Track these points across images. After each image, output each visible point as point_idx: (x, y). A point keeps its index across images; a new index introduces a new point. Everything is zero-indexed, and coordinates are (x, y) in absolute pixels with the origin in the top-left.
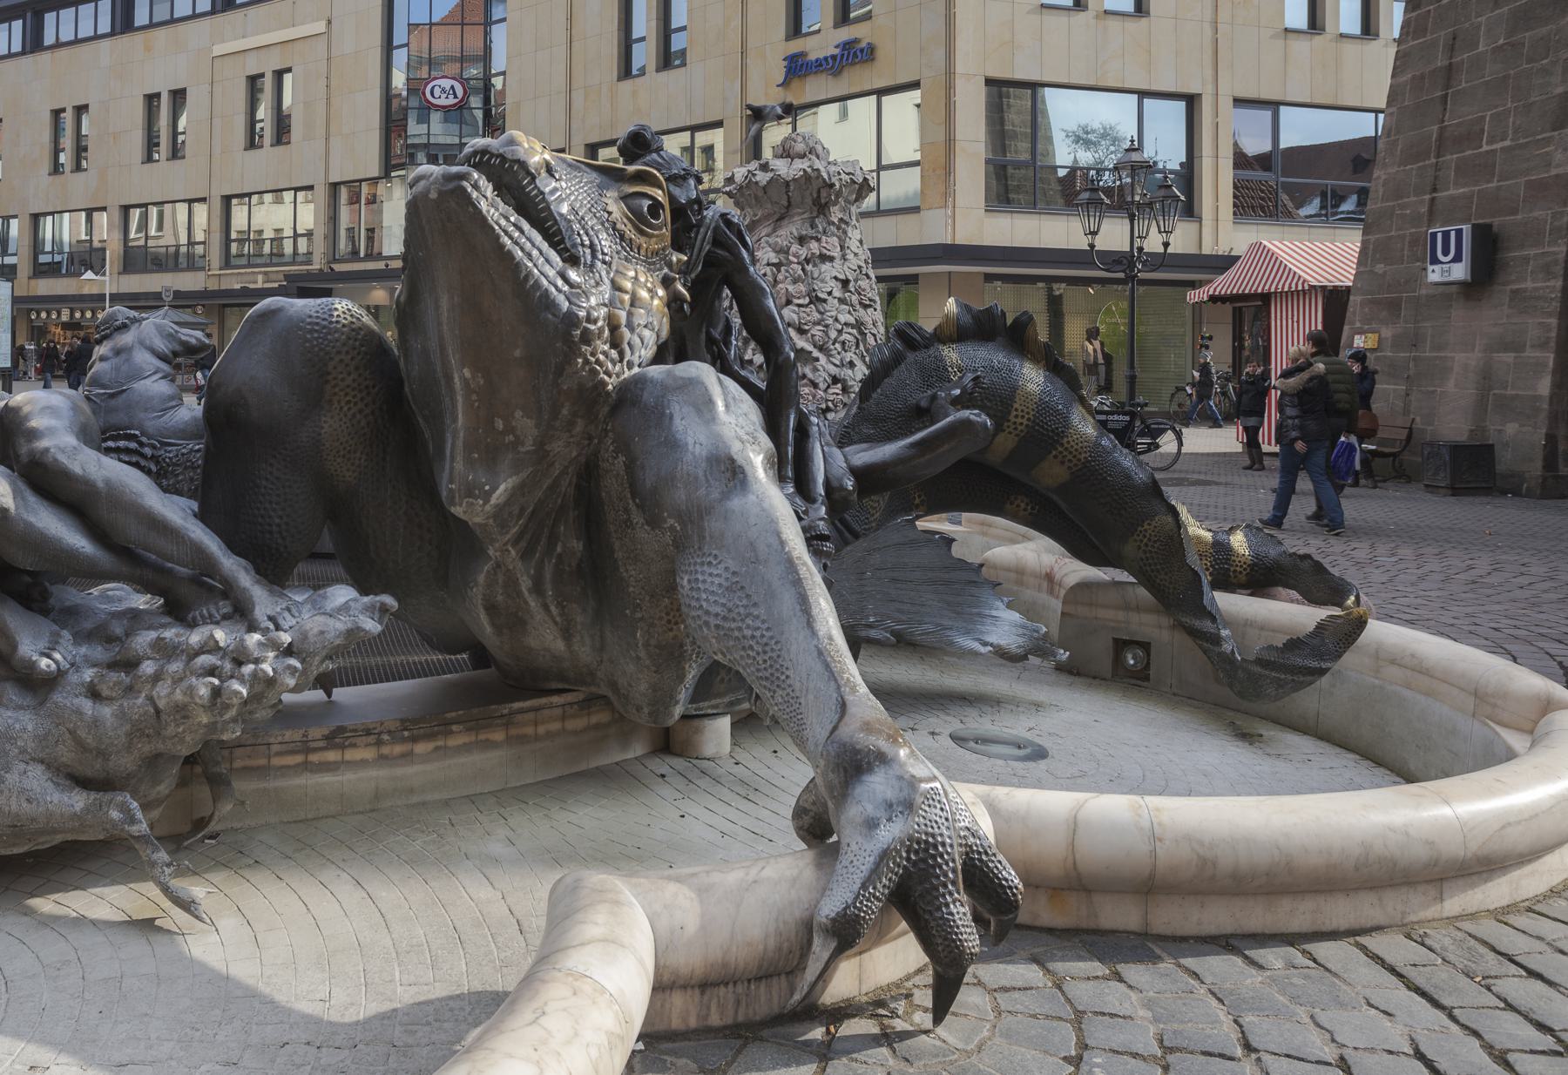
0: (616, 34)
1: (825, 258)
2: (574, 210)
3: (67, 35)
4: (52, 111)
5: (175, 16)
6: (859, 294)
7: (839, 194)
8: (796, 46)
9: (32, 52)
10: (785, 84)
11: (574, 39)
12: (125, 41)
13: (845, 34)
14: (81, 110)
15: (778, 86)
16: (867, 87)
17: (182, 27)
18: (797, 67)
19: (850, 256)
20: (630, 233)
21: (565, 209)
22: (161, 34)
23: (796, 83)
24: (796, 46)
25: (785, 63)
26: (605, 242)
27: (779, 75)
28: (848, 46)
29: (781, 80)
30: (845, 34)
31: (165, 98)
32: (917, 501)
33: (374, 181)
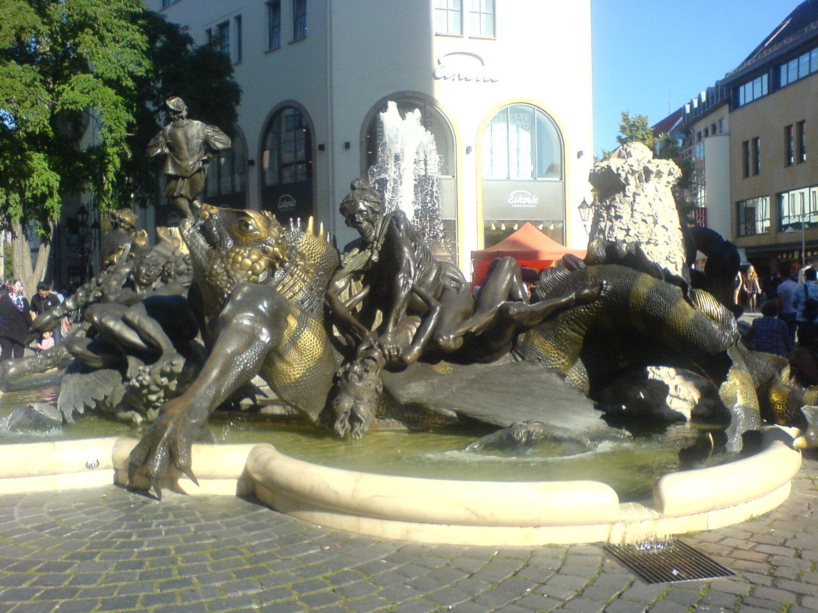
1: (618, 217)
3: (793, 77)
6: (638, 237)
9: (773, 92)
14: (801, 124)
19: (636, 214)
32: (621, 357)
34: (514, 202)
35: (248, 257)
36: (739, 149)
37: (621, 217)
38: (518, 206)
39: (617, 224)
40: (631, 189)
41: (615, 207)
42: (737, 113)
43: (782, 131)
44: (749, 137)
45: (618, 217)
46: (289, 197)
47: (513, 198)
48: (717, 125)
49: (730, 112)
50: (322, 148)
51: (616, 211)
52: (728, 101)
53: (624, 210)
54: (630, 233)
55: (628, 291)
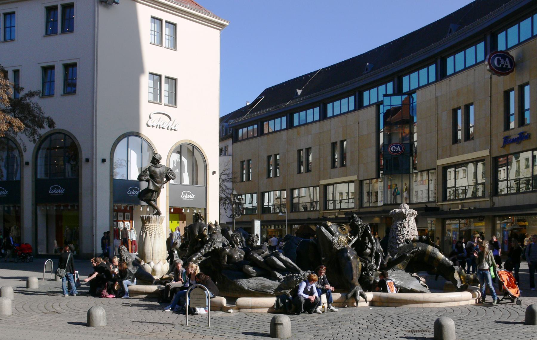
0: (451, 128)
1: (404, 227)
2: (334, 230)
3: (272, 129)
4: (267, 156)
5: (307, 122)
7: (407, 216)
8: (507, 133)
10: (504, 146)
11: (438, 129)
12: (291, 131)
13: (521, 130)
15: (501, 147)
16: (528, 148)
17: (309, 126)
18: (507, 141)
19: (410, 227)
20: (341, 232)
21: (332, 230)
22: (303, 129)
23: (507, 146)
24: (507, 133)
25: (503, 140)
26: (337, 233)
27: (502, 143)
28: (521, 134)
29: (502, 145)
30: (521, 130)
31: (304, 150)
33: (371, 180)
34: (184, 197)
35: (344, 239)
36: (238, 165)
37: (405, 227)
38: (185, 199)
39: (404, 229)
40: (407, 219)
41: (403, 224)
42: (238, 145)
43: (266, 158)
44: (245, 158)
45: (404, 227)
46: (59, 187)
47: (183, 194)
48: (223, 149)
49: (233, 143)
50: (87, 160)
51: (404, 225)
52: (231, 136)
53: (406, 225)
54: (409, 232)
55: (426, 250)
